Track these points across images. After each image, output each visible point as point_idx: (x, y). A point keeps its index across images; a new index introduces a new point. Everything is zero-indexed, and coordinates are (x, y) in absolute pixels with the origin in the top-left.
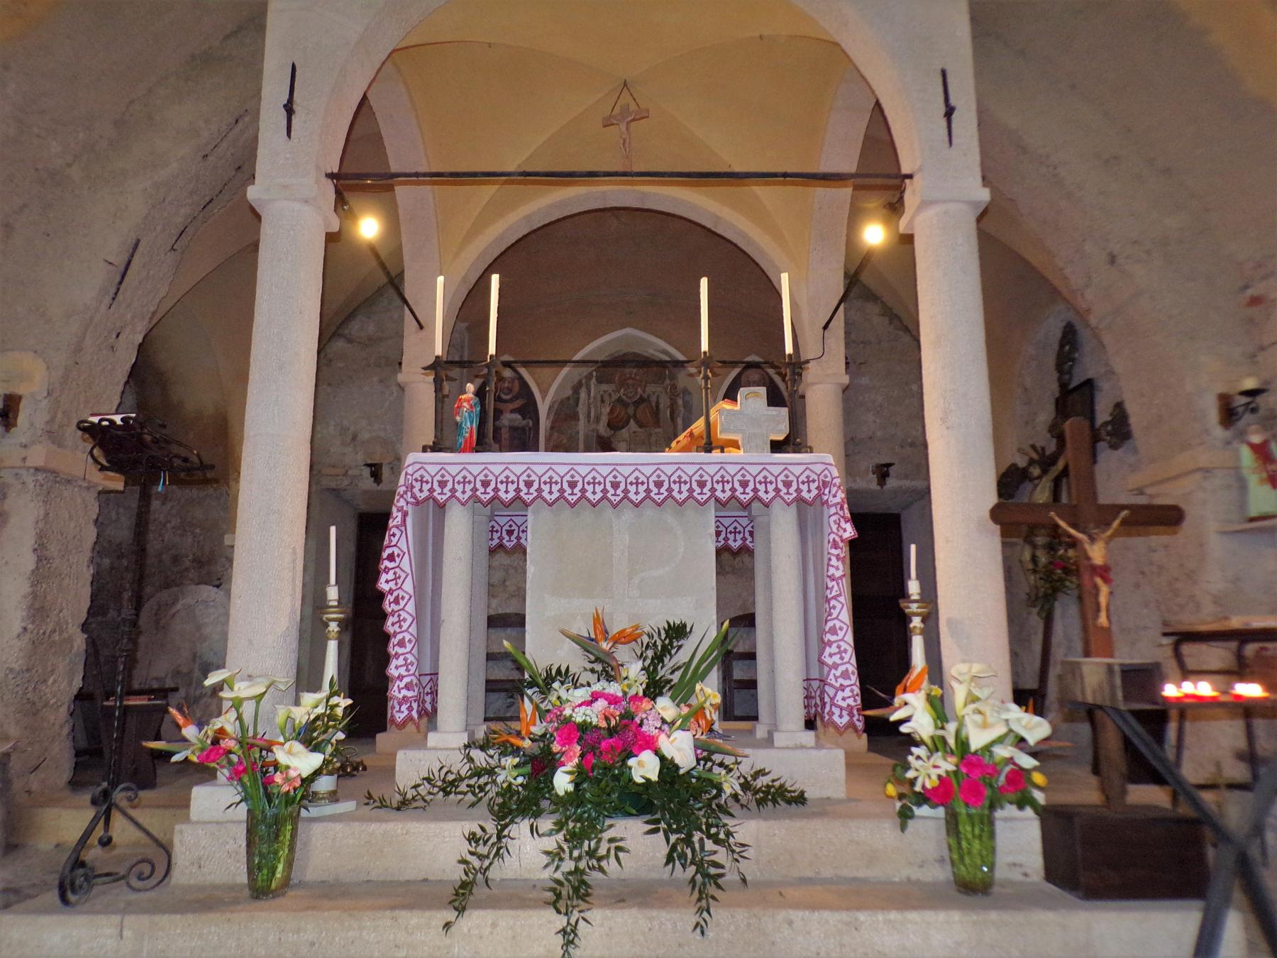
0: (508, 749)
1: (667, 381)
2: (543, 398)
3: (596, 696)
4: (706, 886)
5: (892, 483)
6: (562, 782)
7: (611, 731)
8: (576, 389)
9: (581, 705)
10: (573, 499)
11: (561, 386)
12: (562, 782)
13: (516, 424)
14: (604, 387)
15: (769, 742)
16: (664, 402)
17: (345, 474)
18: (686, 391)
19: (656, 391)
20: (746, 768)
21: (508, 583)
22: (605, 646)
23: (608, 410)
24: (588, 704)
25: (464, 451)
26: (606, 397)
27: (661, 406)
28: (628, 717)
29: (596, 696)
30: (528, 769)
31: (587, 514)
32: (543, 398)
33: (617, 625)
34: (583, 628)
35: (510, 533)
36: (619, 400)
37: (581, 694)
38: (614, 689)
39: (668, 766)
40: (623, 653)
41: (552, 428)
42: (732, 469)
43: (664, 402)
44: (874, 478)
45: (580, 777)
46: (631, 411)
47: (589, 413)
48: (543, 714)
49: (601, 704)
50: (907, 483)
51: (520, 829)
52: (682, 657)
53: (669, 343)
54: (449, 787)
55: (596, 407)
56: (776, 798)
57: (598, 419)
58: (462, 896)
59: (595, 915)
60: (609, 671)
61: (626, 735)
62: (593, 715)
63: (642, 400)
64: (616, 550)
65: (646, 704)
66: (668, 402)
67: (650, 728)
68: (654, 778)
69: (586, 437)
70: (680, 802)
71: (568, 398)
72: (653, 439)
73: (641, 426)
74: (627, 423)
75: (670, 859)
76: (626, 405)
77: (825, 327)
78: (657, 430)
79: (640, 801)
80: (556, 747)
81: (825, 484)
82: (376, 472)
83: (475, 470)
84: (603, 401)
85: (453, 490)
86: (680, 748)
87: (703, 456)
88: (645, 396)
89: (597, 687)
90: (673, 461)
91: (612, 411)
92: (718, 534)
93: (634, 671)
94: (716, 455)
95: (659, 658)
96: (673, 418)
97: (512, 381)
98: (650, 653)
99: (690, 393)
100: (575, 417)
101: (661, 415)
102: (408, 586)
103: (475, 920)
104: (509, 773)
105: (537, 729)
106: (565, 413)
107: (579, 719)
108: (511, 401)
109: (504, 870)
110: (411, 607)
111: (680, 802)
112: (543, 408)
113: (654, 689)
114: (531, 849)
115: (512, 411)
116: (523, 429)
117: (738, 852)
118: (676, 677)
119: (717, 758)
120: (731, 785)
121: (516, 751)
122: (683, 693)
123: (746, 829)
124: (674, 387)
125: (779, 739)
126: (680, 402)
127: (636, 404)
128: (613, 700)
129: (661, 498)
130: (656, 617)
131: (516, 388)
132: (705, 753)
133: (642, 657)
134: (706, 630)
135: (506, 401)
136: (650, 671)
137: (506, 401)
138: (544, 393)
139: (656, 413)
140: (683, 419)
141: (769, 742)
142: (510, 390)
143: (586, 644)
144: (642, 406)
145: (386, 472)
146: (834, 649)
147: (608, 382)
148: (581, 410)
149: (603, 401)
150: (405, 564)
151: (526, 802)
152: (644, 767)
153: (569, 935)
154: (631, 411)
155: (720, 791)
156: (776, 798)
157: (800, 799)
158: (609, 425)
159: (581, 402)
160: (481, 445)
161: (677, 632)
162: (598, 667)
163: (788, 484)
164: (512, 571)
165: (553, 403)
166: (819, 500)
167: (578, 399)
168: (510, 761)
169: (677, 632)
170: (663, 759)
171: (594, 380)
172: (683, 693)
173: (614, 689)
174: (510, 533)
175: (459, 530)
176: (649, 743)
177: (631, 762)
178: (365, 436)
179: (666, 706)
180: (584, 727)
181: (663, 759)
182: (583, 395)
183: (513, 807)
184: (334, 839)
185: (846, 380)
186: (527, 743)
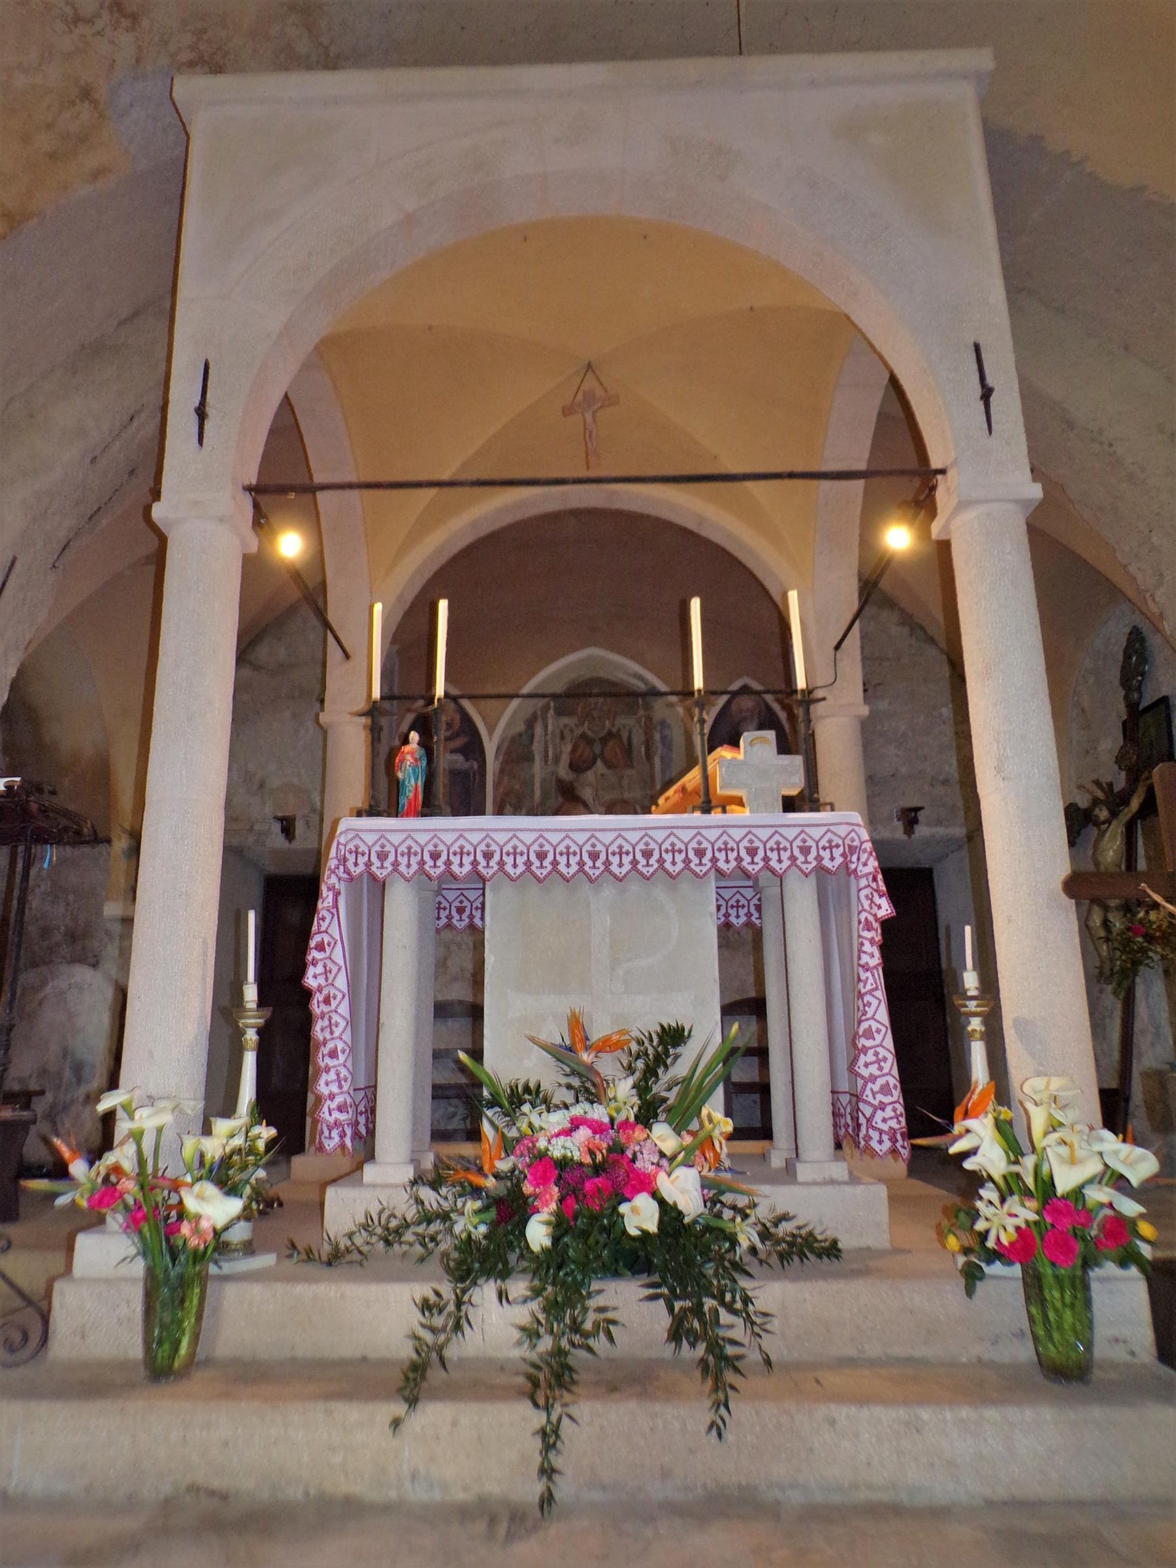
1: (641, 712)
2: (491, 734)
3: (576, 1123)
4: (719, 1368)
6: (538, 1234)
7: (598, 1169)
8: (530, 723)
9: (558, 1134)
10: (543, 874)
12: (538, 1234)
13: (458, 766)
14: (565, 720)
15: (788, 1173)
16: (638, 738)
18: (663, 723)
19: (627, 723)
20: (762, 1212)
21: (449, 963)
22: (586, 1057)
23: (569, 748)
24: (567, 1133)
25: (407, 814)
26: (566, 732)
27: (635, 741)
28: (617, 1150)
29: (576, 1123)
30: (492, 1214)
31: (559, 891)
32: (491, 734)
34: (556, 1033)
35: (460, 910)
36: (583, 736)
37: (557, 1120)
38: (599, 1113)
39: (669, 1212)
40: (607, 1066)
41: (502, 771)
42: (737, 834)
43: (638, 738)
44: (899, 826)
45: (560, 1228)
46: (597, 748)
47: (546, 751)
48: (508, 1146)
49: (584, 1133)
51: (485, 1293)
52: (680, 1069)
53: (646, 666)
54: (392, 1236)
56: (805, 1251)
57: (557, 760)
59: (584, 1409)
60: (590, 1088)
61: (615, 1173)
62: (573, 1147)
63: (610, 735)
64: (598, 936)
65: (639, 1133)
66: (643, 738)
67: (645, 1163)
68: (652, 1227)
69: (544, 781)
71: (520, 735)
72: (625, 783)
73: (609, 765)
74: (594, 763)
75: (675, 1335)
76: (590, 742)
77: (837, 647)
78: (630, 772)
79: (633, 1257)
80: (528, 1188)
81: (852, 849)
82: (288, 827)
83: (423, 838)
84: (562, 737)
85: (396, 864)
86: (684, 1189)
87: (697, 817)
88: (614, 730)
89: (577, 1111)
90: (661, 825)
91: (574, 751)
92: (719, 908)
93: (624, 1089)
94: (716, 817)
95: (651, 1072)
96: (649, 756)
98: (640, 1064)
99: (669, 727)
100: (529, 758)
101: (635, 754)
102: (341, 982)
103: (432, 1416)
104: (471, 1222)
105: (503, 1166)
106: (518, 752)
107: (556, 1153)
110: (344, 1009)
111: (684, 1258)
113: (647, 1114)
114: (500, 1319)
118: (672, 1096)
119: (727, 1198)
120: (747, 1236)
121: (476, 1191)
122: (683, 1115)
123: (770, 1293)
124: (649, 718)
125: (804, 1172)
126: (657, 736)
127: (604, 741)
128: (597, 1128)
129: (653, 871)
130: (646, 1016)
133: (630, 1070)
134: (708, 1034)
136: (642, 1088)
138: (491, 729)
139: (628, 750)
140: (662, 758)
141: (788, 1173)
143: (563, 1054)
144: (611, 743)
145: (300, 827)
146: (870, 1057)
147: (570, 714)
148: (537, 747)
149: (562, 737)
150: (338, 955)
152: (639, 1215)
154: (597, 748)
155: (734, 1242)
157: (832, 1250)
158: (572, 766)
160: (428, 807)
161: (673, 1036)
162: (576, 1082)
163: (805, 851)
164: (454, 948)
165: (502, 740)
166: (847, 871)
167: (532, 736)
168: (472, 1205)
169: (673, 1036)
170: (662, 1202)
171: (551, 712)
172: (683, 1115)
173: (599, 1113)
174: (460, 910)
176: (645, 1184)
177: (624, 1208)
178: (275, 782)
179: (663, 1136)
180: (564, 1164)
181: (662, 1202)
182: (538, 730)
184: (252, 1308)
185: (865, 711)
186: (490, 1182)
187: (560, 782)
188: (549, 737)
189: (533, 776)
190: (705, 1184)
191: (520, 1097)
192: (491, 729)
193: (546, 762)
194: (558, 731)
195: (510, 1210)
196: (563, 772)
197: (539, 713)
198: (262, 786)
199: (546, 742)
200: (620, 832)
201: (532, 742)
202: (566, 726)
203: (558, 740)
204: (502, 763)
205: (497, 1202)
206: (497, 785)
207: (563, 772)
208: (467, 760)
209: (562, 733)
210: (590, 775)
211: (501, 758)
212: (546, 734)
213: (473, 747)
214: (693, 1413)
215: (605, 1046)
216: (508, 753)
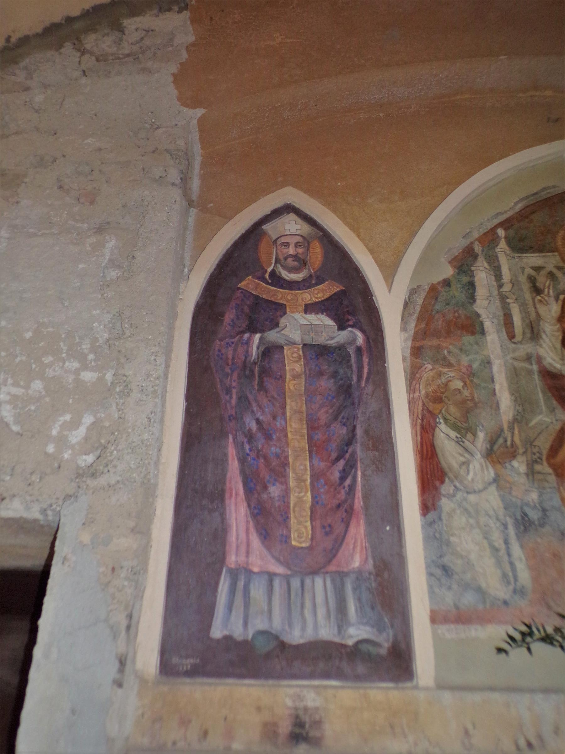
11: (425, 260)
13: (322, 339)
14: (533, 259)
26: (542, 280)
41: (417, 351)
55: (523, 306)
57: (534, 332)
69: (514, 375)
71: (447, 283)
97: (306, 242)
100: (473, 326)
106: (445, 319)
108: (305, 284)
112: (390, 304)
115: (309, 308)
116: (341, 347)
131: (317, 254)
135: (291, 285)
137: (291, 285)
142: (302, 263)
149: (537, 291)
159: (481, 292)
165: (413, 292)
167: (472, 285)
171: (503, 245)
182: (482, 276)
187: (549, 375)
188: (507, 288)
189: (488, 363)
192: (389, 272)
193: (511, 336)
194: (523, 279)
197: (477, 248)
199: (503, 298)
201: (472, 298)
202: (538, 269)
203: (528, 296)
204: (415, 338)
206: (412, 377)
208: (341, 327)
209: (532, 280)
211: (412, 325)
212: (500, 286)
213: (352, 303)
216: (426, 316)
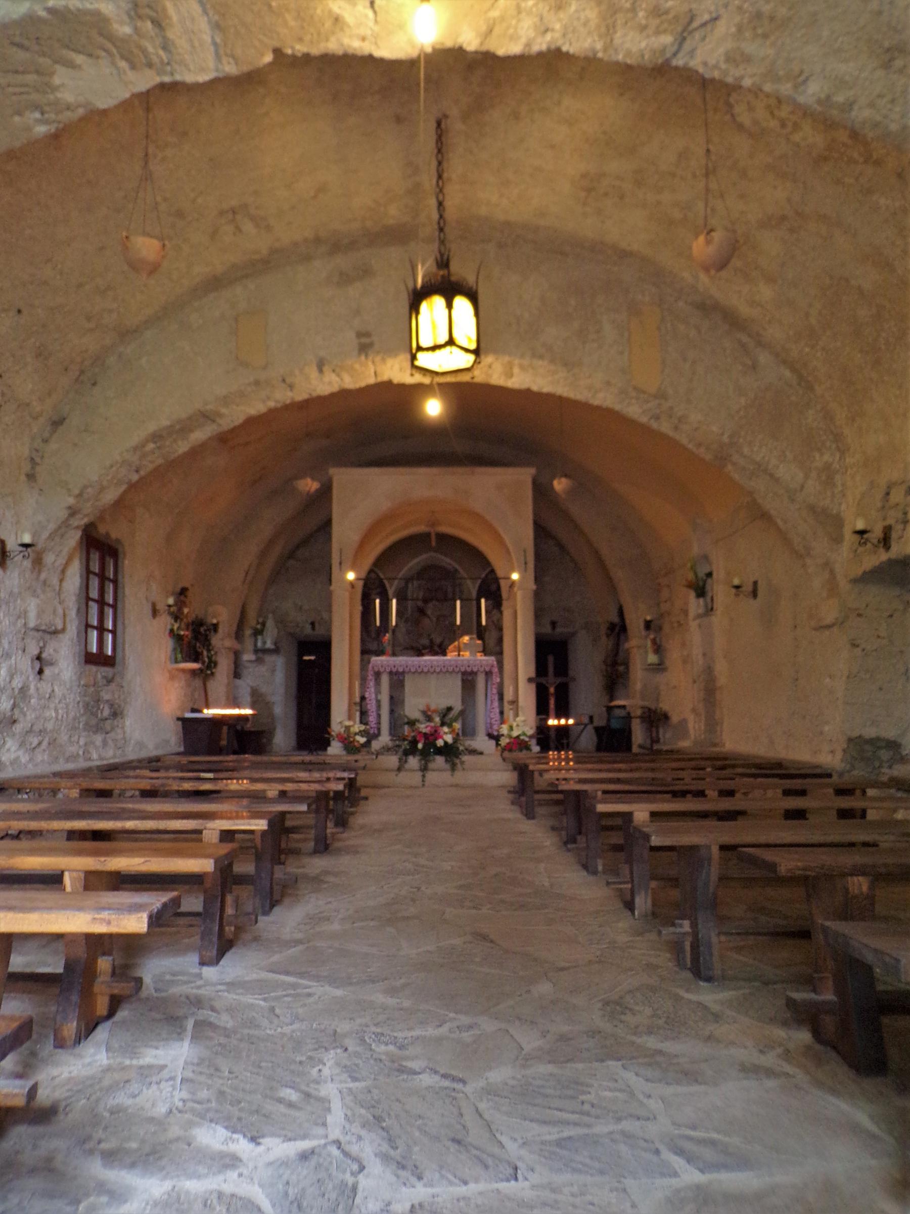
0: (404, 740)
4: (453, 768)
5: (559, 630)
6: (420, 746)
9: (424, 728)
10: (420, 672)
12: (420, 746)
16: (450, 589)
17: (298, 626)
28: (436, 731)
33: (433, 707)
34: (422, 707)
37: (423, 726)
38: (432, 724)
39: (446, 743)
45: (425, 745)
50: (566, 630)
52: (451, 716)
56: (473, 752)
58: (399, 769)
59: (430, 772)
60: (429, 719)
61: (435, 734)
67: (442, 733)
70: (450, 752)
79: (439, 751)
82: (313, 624)
86: (449, 738)
93: (437, 720)
103: (402, 774)
105: (413, 734)
109: (407, 766)
111: (450, 752)
113: (443, 724)
114: (414, 762)
117: (462, 763)
120: (461, 748)
122: (450, 726)
128: (432, 727)
129: (445, 671)
130: (443, 704)
132: (456, 740)
134: (458, 707)
138: (391, 585)
145: (317, 625)
151: (412, 750)
152: (440, 743)
153: (424, 776)
156: (473, 752)
157: (481, 753)
161: (449, 709)
168: (406, 742)
173: (432, 724)
175: (385, 680)
176: (441, 737)
179: (446, 729)
180: (425, 734)
182: (410, 585)
183: (407, 753)
190: (454, 739)
191: (412, 723)
195: (414, 742)
196: (420, 603)
198: (301, 608)
200: (437, 661)
205: (410, 742)
207: (420, 603)
210: (430, 605)
214: (449, 773)
215: (435, 711)
